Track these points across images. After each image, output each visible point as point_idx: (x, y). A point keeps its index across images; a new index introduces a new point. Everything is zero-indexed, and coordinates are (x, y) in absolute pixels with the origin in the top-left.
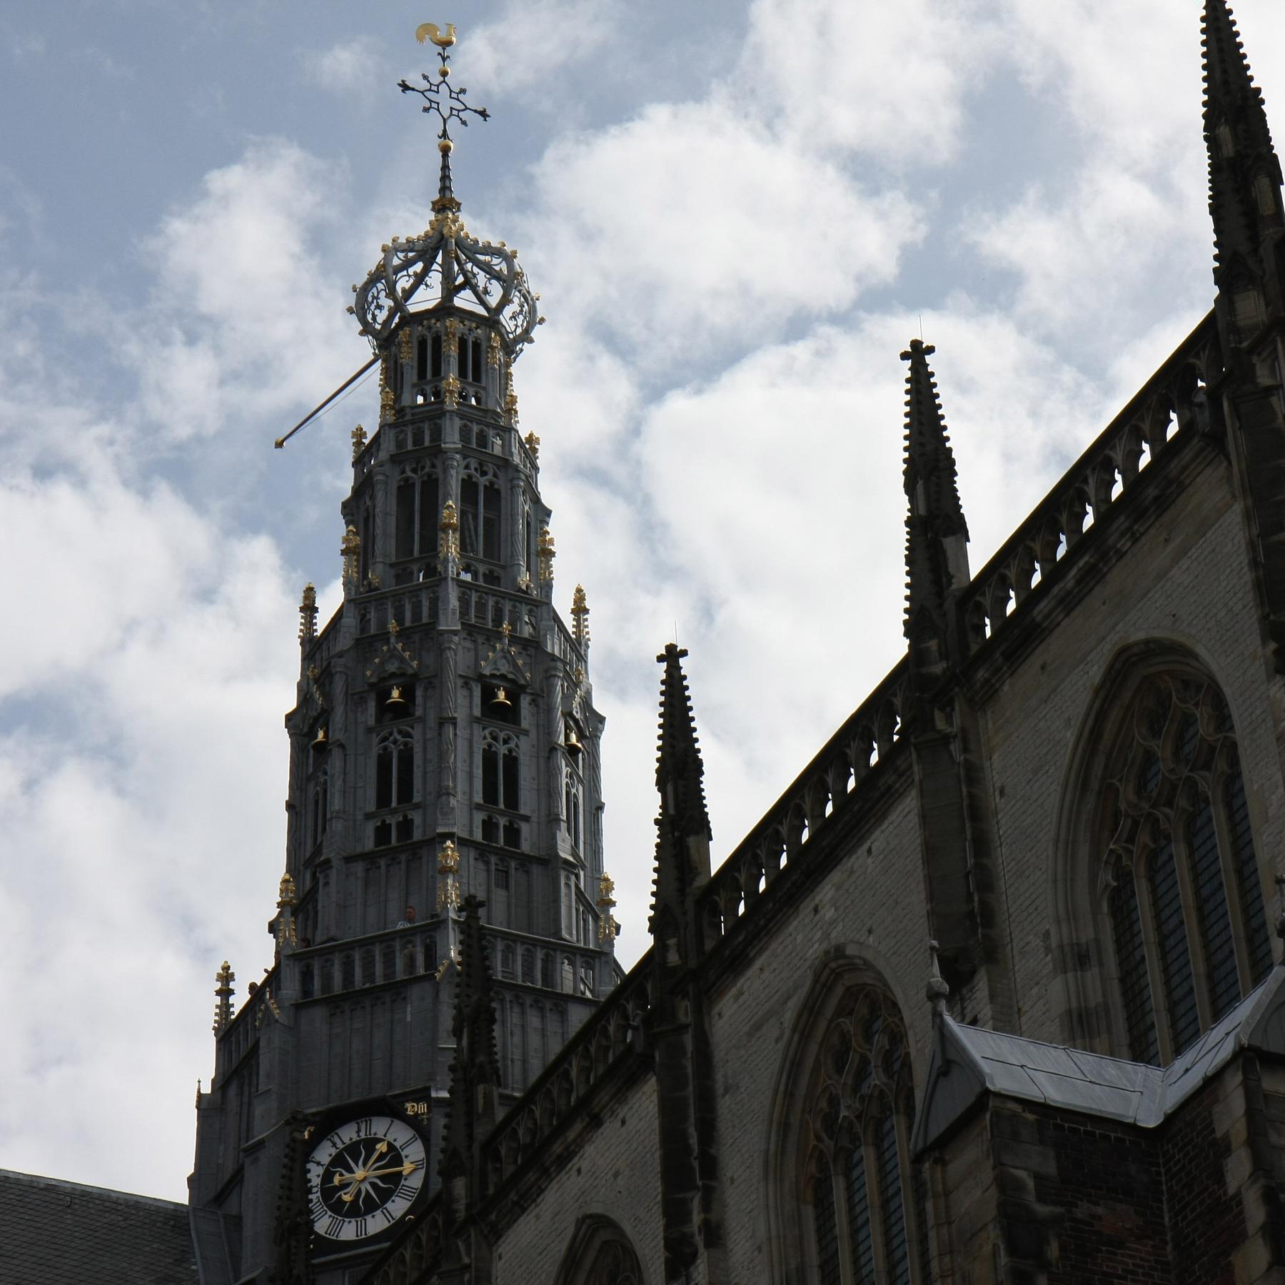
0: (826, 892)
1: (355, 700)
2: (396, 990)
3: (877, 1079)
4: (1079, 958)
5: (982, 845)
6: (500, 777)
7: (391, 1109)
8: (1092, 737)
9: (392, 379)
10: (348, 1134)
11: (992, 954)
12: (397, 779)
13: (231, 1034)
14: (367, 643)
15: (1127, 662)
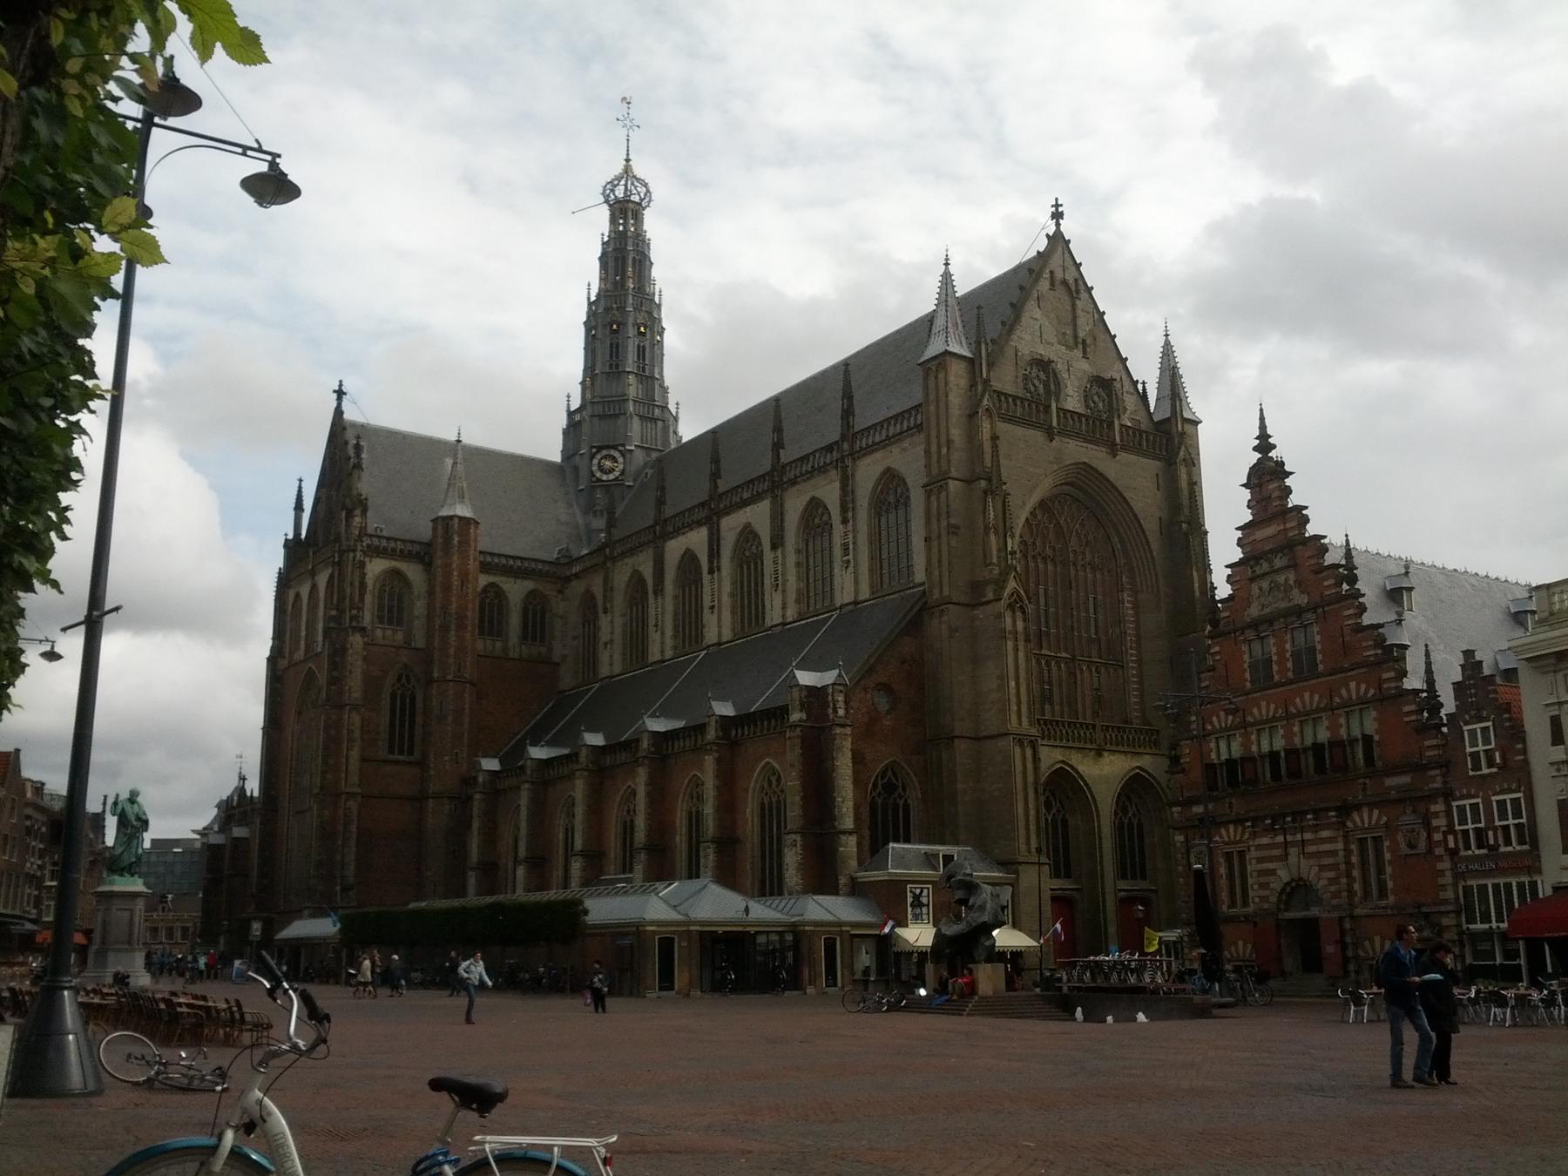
0: (748, 509)
1: (604, 326)
2: (616, 416)
3: (754, 549)
4: (798, 551)
5: (782, 520)
6: (641, 351)
7: (615, 447)
8: (805, 510)
9: (613, 220)
10: (604, 452)
11: (782, 545)
12: (616, 351)
13: (570, 414)
14: (608, 309)
15: (813, 498)
